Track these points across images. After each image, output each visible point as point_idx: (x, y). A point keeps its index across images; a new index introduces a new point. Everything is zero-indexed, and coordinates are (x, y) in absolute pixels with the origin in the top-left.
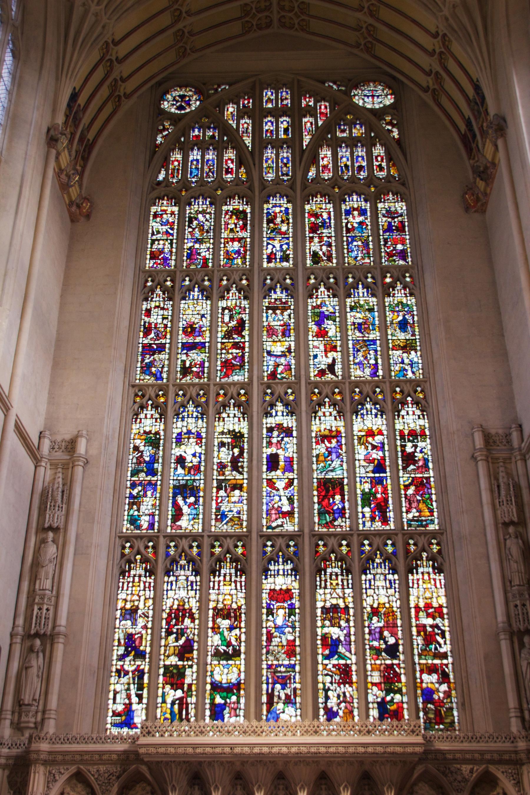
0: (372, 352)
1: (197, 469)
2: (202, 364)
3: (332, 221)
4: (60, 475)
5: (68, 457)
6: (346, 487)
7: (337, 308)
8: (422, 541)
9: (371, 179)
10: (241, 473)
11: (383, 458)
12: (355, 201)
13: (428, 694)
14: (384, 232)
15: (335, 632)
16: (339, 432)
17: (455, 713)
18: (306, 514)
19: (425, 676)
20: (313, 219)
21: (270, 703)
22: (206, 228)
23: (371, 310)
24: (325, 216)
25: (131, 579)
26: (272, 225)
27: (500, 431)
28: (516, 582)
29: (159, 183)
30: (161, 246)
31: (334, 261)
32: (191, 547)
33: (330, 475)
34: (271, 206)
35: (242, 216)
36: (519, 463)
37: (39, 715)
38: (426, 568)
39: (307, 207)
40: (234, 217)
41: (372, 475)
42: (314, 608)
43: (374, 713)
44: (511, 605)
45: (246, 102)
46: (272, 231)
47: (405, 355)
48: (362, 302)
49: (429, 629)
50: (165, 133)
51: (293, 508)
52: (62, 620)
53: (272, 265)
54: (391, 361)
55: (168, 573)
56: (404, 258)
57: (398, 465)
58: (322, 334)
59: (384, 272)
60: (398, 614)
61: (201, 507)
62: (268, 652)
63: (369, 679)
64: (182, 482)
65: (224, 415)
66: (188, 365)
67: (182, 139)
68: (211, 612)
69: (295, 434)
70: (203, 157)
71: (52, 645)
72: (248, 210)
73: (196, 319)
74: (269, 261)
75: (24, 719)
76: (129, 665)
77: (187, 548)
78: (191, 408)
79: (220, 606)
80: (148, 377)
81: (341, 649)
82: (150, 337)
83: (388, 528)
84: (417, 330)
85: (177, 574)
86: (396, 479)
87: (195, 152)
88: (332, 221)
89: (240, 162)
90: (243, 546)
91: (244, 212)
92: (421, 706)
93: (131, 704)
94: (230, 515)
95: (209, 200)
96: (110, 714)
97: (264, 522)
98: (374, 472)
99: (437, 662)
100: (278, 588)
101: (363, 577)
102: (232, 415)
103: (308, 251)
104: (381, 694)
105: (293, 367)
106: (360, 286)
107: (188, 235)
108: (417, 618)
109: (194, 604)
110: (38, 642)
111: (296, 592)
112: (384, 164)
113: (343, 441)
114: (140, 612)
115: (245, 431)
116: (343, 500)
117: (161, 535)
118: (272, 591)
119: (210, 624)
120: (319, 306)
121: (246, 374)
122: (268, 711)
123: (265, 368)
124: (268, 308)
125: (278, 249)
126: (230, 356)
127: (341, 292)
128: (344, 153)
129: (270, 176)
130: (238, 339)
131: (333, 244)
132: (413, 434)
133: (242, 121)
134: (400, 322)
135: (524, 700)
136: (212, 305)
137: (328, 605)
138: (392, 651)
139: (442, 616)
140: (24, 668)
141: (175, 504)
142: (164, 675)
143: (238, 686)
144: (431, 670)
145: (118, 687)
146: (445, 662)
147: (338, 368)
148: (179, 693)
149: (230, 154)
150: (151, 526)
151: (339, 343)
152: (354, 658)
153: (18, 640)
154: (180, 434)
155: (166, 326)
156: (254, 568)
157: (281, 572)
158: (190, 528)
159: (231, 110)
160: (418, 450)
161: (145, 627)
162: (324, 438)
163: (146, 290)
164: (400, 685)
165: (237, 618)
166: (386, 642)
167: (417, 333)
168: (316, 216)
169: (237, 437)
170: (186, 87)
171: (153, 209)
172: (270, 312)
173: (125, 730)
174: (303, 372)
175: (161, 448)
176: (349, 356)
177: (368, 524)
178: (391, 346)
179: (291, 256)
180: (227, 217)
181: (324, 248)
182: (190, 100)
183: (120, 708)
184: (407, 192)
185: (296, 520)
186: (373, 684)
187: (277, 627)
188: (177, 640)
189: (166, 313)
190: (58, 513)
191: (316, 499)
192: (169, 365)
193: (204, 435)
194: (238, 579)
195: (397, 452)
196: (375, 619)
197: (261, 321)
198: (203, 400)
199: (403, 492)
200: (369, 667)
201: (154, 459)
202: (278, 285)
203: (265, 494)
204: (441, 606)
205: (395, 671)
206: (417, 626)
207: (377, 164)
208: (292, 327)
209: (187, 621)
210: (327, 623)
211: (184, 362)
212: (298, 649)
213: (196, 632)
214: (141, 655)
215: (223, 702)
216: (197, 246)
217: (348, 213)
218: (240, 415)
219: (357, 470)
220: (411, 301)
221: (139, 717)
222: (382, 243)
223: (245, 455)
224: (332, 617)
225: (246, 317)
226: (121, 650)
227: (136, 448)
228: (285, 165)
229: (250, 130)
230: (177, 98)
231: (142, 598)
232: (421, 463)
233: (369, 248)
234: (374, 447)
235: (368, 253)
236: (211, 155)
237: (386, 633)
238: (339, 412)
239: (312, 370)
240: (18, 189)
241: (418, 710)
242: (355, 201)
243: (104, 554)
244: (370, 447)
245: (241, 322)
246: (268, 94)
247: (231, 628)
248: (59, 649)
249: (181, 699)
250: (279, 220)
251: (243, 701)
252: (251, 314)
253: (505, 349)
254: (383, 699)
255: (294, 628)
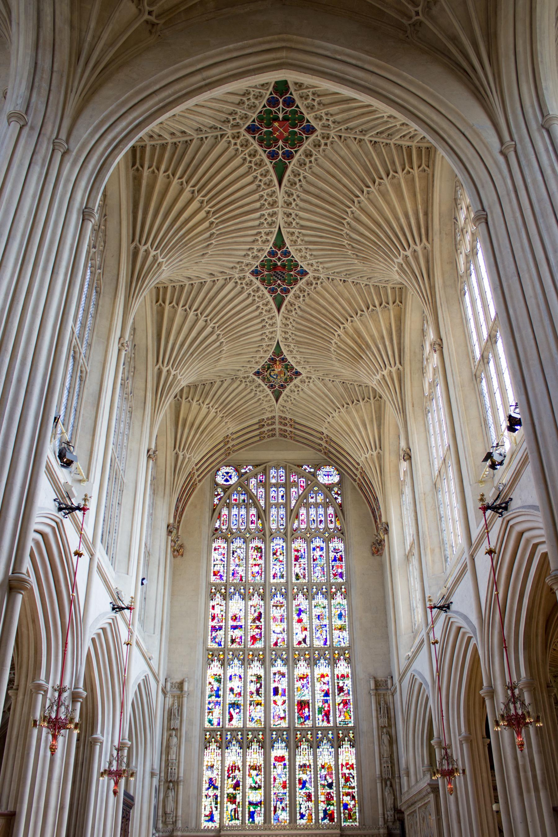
0: (324, 632)
1: (240, 694)
2: (241, 638)
3: (306, 555)
4: (176, 701)
5: (179, 692)
6: (311, 705)
7: (308, 606)
8: (345, 732)
9: (327, 529)
10: (261, 697)
11: (328, 690)
12: (318, 542)
13: (346, 806)
14: (332, 561)
15: (305, 777)
16: (307, 675)
17: (357, 814)
18: (292, 720)
19: (345, 797)
20: (296, 553)
21: (275, 811)
22: (241, 557)
23: (324, 607)
24: (302, 551)
25: (210, 751)
26: (275, 556)
27: (383, 679)
28: (385, 756)
29: (216, 530)
30: (218, 569)
31: (307, 578)
32: (238, 735)
33: (303, 698)
34: (274, 545)
35: (260, 550)
36: (390, 696)
37: (174, 818)
38: (346, 745)
39: (293, 546)
40: (256, 551)
41: (323, 698)
42: (295, 765)
43: (321, 815)
44: (383, 766)
45: (261, 477)
46: (275, 560)
47: (341, 633)
48: (320, 603)
49: (347, 775)
50: (219, 497)
51: (285, 715)
52: (181, 774)
53: (275, 581)
54: (334, 637)
55: (227, 748)
56: (342, 578)
57: (335, 693)
58: (300, 621)
59: (331, 585)
60: (333, 768)
61: (242, 715)
62: (274, 787)
63: (320, 799)
64: (233, 702)
65: (252, 666)
66: (234, 638)
67: (228, 501)
68: (248, 768)
69: (286, 676)
70: (239, 512)
71: (178, 785)
72: (263, 547)
73: (237, 612)
74: (274, 578)
75: (167, 820)
76: (211, 792)
77: (236, 735)
78: (236, 661)
79: (252, 764)
80: (214, 644)
81: (307, 785)
82: (214, 621)
83: (329, 725)
84: (347, 619)
85: (231, 748)
86: (334, 700)
87: (235, 509)
88: (306, 555)
89: (259, 518)
90: (262, 735)
91: (260, 548)
92: (342, 811)
93: (212, 811)
94: (256, 719)
95: (242, 540)
96: (203, 815)
97: (272, 722)
98: (324, 696)
99: (350, 791)
100: (278, 756)
101: (318, 750)
102: (256, 666)
103: (293, 572)
104: (325, 806)
105: (286, 639)
106: (319, 594)
107: (232, 562)
108: (342, 770)
109: (239, 764)
110: (171, 785)
111: (287, 757)
112: (333, 520)
113: (310, 680)
114: (215, 767)
115: (262, 675)
116: (309, 711)
117: (224, 729)
118: (276, 757)
119: (247, 773)
120: (299, 605)
121: (263, 643)
122: (274, 814)
123: (272, 640)
124: (273, 606)
125: (278, 570)
126: (255, 634)
127: (310, 597)
128: (312, 511)
129: (274, 526)
130: (258, 623)
131: (306, 568)
132: (343, 676)
133: (259, 490)
134: (338, 615)
135: (385, 810)
136: (245, 603)
137: (301, 764)
138: (330, 786)
139: (353, 769)
140: (166, 797)
141: (230, 713)
142: (227, 797)
143: (260, 802)
144: (348, 794)
145: (206, 803)
146: (354, 790)
147: (308, 640)
148: (234, 806)
149: (253, 511)
150: (219, 724)
151: (308, 627)
152: (313, 789)
153: (162, 783)
154: (231, 676)
155: (222, 616)
156: (268, 745)
157: (280, 748)
158: (237, 725)
159: (253, 482)
160: (345, 685)
161: (218, 774)
162: (302, 678)
163: (212, 594)
164: (333, 802)
165: (260, 770)
166: (327, 782)
167: (347, 621)
168: (297, 551)
169: (259, 678)
170: (229, 466)
171: (214, 545)
172: (274, 608)
173: (210, 823)
174: (290, 645)
175: (222, 683)
176: (313, 634)
177: (321, 723)
178: (334, 628)
179: (285, 575)
180: (252, 551)
181: (302, 571)
182: (231, 476)
183: (207, 813)
184: (344, 538)
185: (287, 721)
186: (321, 801)
187: (278, 775)
188: (232, 781)
189: (222, 607)
190: (177, 721)
191: (296, 711)
192: (225, 638)
193: (242, 676)
194: (260, 751)
195: (335, 686)
196: (323, 770)
197: (269, 614)
198: (242, 657)
199: (337, 707)
200: (319, 794)
201: (218, 689)
202: (278, 592)
203: (272, 708)
204: (353, 764)
205: (331, 796)
206: (342, 774)
207: (330, 519)
208: (285, 617)
209: (237, 771)
210: (301, 772)
211: (232, 636)
212: (288, 785)
213: (241, 777)
214: (216, 788)
215: (254, 810)
216: (237, 568)
217: (314, 549)
218: (260, 666)
219: (316, 696)
220: (345, 602)
221: (217, 817)
222: (331, 568)
223: (263, 687)
224: (303, 770)
225: (262, 611)
226: (207, 786)
227: (210, 683)
228: (282, 518)
229: (263, 496)
230: (225, 474)
231: (216, 760)
232: (346, 692)
233: (324, 571)
234: (324, 683)
235: (324, 574)
236: (243, 512)
237: (328, 777)
238: (308, 665)
239: (294, 641)
240: (157, 568)
241: (340, 813)
242: (318, 542)
243: (198, 740)
244: (322, 683)
245: (260, 614)
246: (273, 472)
247: (257, 775)
248: (181, 787)
249: (235, 809)
250: (278, 554)
251: (263, 809)
252: (265, 610)
253: (388, 635)
254: (326, 808)
255: (286, 775)
